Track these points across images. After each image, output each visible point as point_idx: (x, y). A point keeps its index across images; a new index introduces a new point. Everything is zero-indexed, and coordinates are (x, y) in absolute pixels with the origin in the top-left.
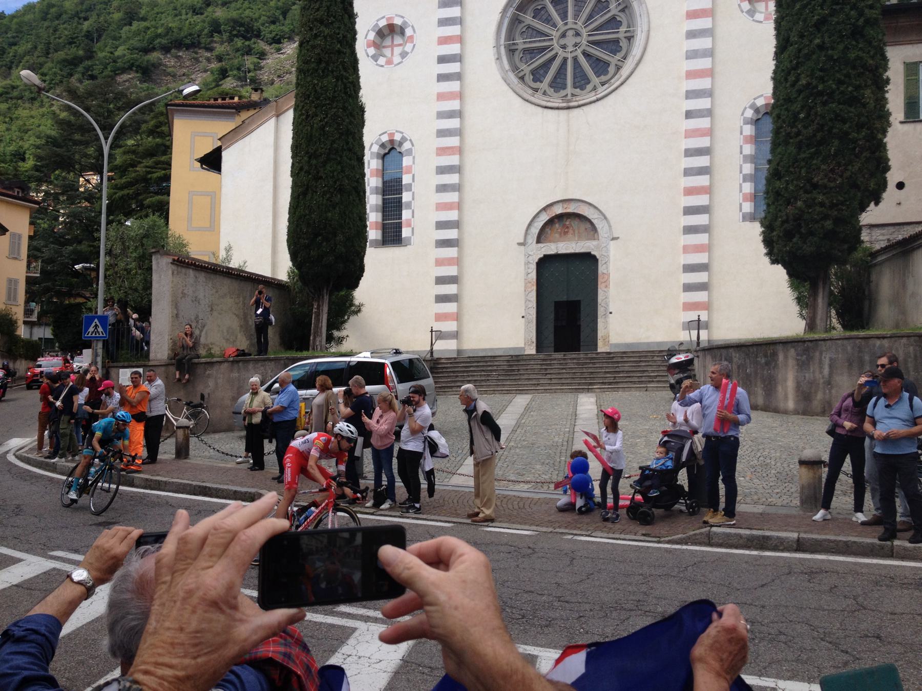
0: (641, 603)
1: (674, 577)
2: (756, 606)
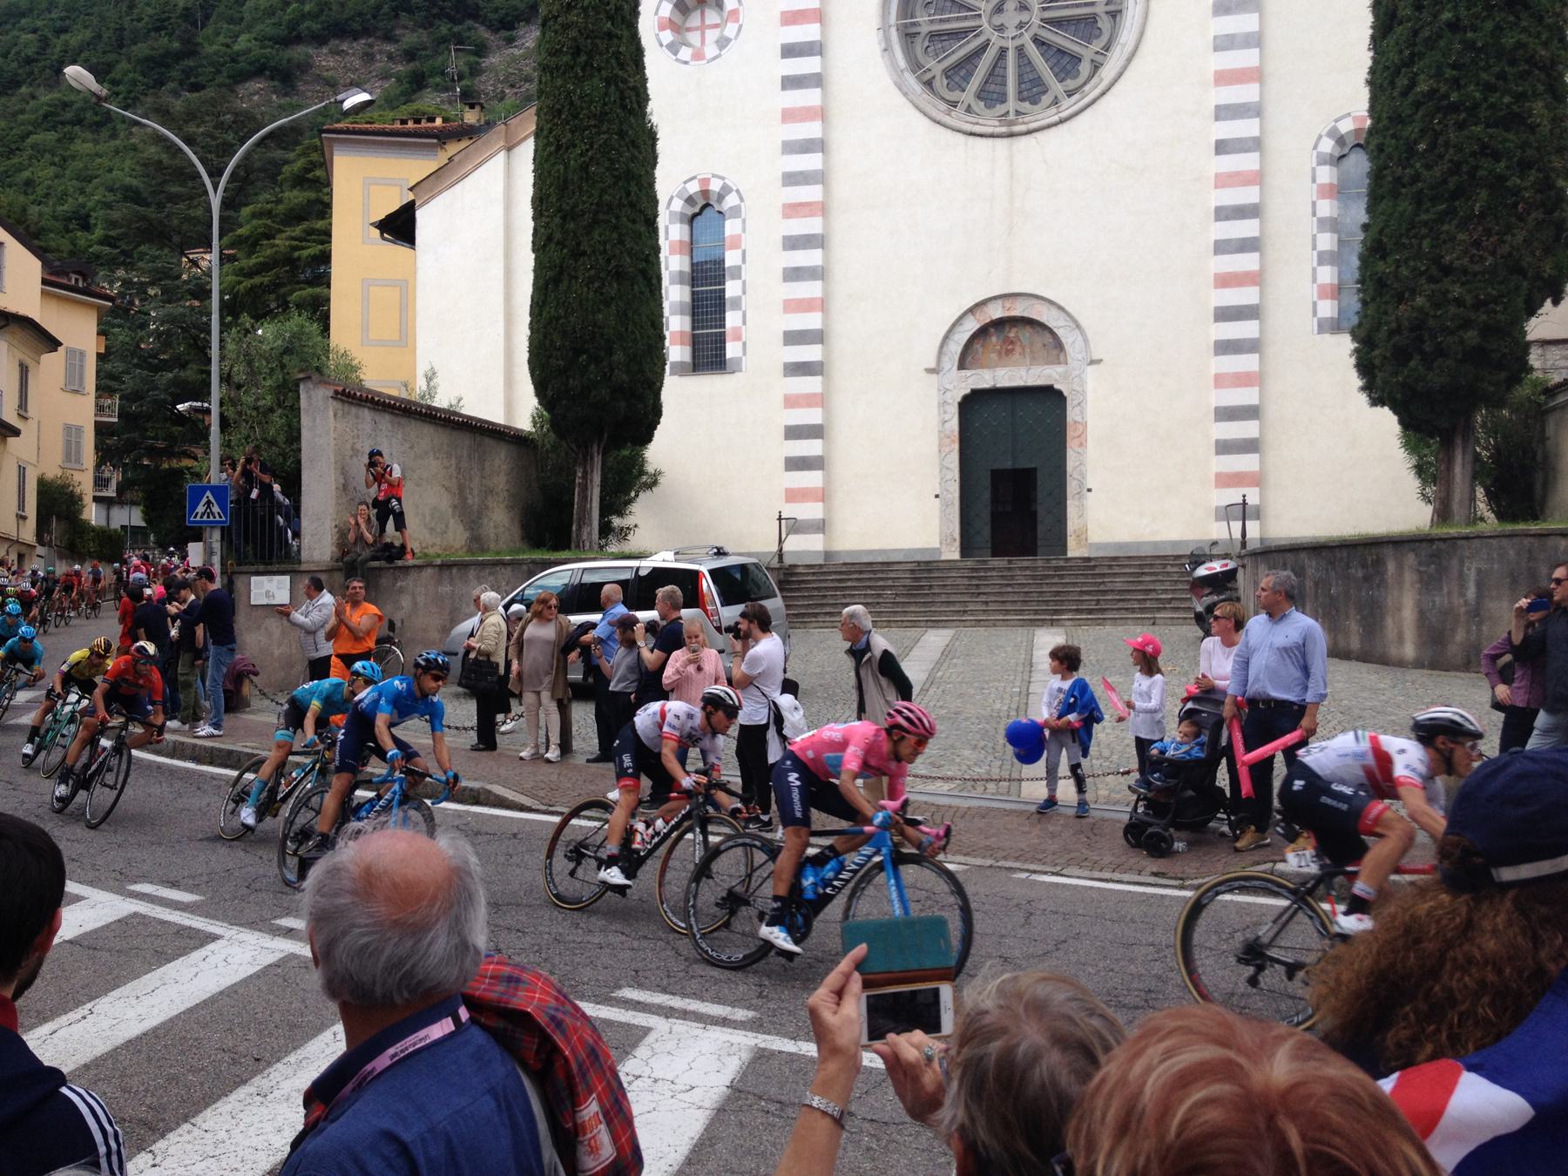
0: (1153, 996)
1: (1211, 949)
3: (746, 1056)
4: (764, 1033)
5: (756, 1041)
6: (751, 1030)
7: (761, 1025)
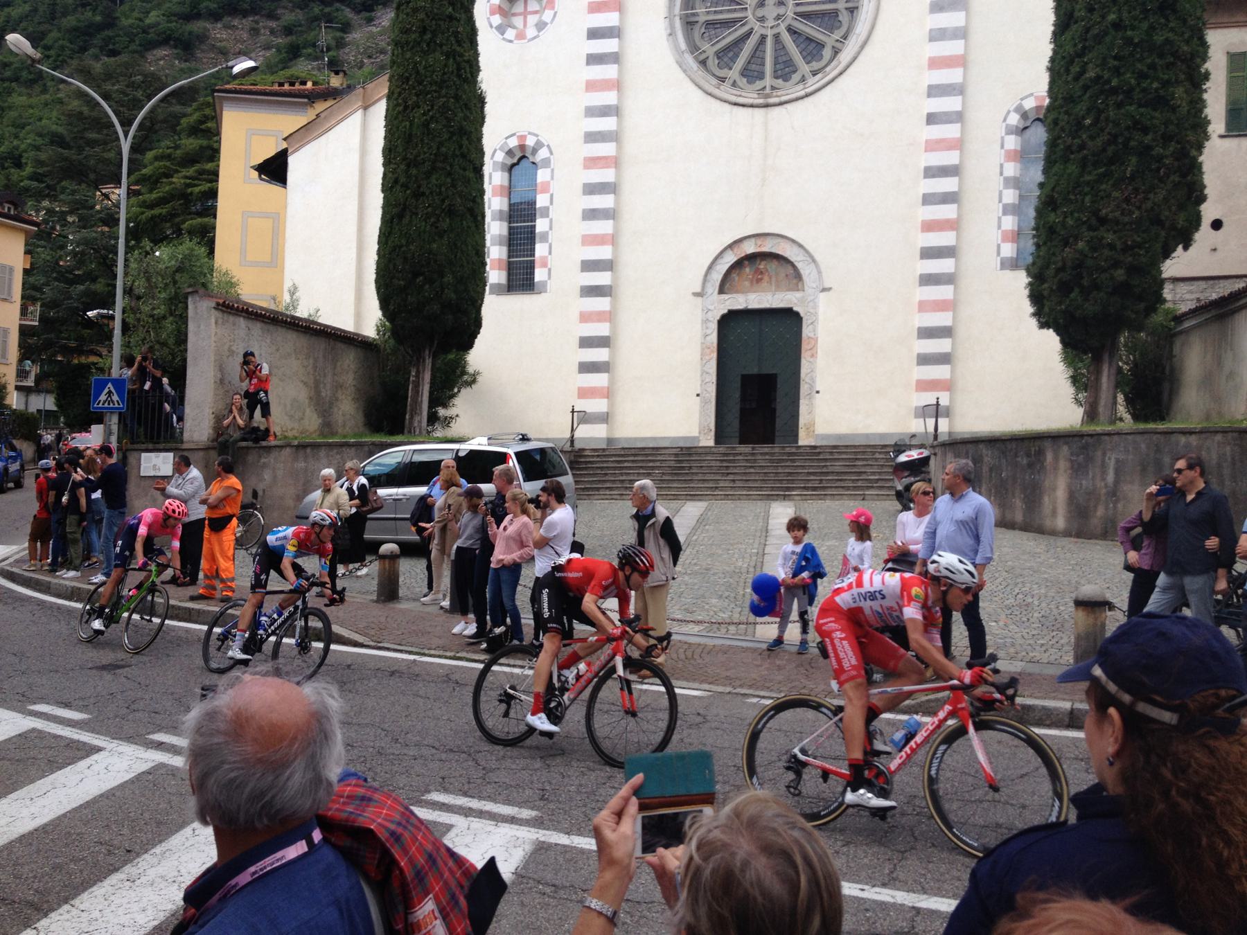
2: (1012, 805)
3: (528, 848)
4: (544, 829)
5: (537, 836)
6: (534, 826)
7: (542, 823)
